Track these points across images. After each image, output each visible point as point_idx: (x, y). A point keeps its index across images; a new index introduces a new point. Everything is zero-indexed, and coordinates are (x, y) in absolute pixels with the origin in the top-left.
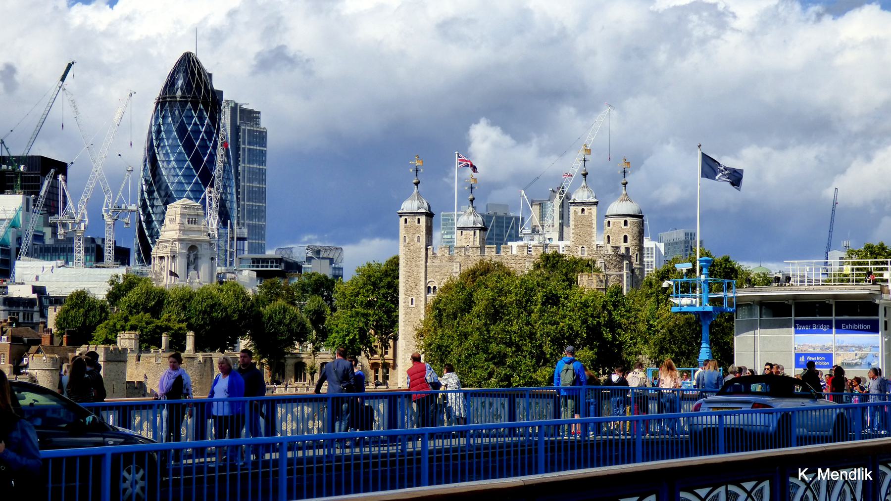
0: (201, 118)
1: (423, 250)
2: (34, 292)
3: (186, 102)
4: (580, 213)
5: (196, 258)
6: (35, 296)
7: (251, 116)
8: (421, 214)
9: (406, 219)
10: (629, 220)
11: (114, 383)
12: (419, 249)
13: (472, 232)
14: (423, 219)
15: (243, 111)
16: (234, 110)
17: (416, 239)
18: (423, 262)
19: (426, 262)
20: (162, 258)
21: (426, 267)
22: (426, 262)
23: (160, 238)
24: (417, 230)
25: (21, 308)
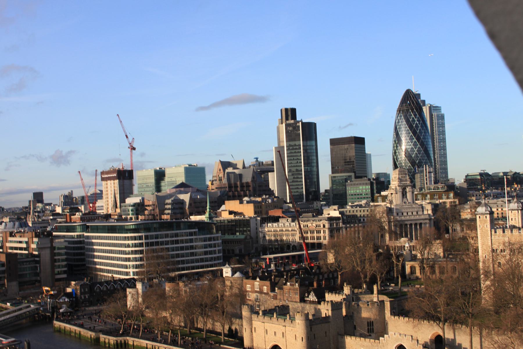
1: (489, 232)
2: (340, 214)
3: (409, 110)
6: (340, 216)
7: (437, 109)
8: (487, 214)
9: (480, 217)
11: (337, 320)
12: (487, 231)
13: (517, 211)
14: (488, 216)
15: (434, 107)
16: (430, 108)
17: (485, 226)
18: (490, 238)
19: (491, 237)
20: (392, 194)
21: (491, 240)
22: (491, 237)
24: (485, 222)
25: (335, 221)
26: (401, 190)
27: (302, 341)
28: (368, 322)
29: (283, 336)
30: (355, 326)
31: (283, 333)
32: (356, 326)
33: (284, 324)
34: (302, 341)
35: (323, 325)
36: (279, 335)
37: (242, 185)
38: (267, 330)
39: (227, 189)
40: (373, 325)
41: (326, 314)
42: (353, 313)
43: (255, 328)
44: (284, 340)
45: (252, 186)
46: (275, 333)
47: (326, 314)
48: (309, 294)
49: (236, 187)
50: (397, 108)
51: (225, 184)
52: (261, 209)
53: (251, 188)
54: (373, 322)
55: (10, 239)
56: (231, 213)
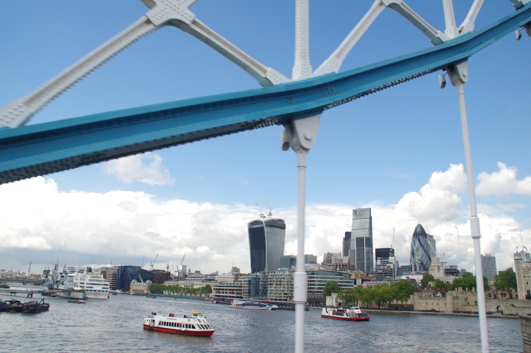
0: (423, 238)
5: (439, 270)
6: (407, 279)
20: (432, 270)
23: (431, 265)
26: (437, 268)
28: (475, 301)
29: (437, 304)
30: (469, 303)
31: (437, 303)
32: (469, 303)
33: (438, 299)
36: (435, 304)
38: (427, 303)
39: (335, 267)
41: (457, 296)
42: (467, 297)
43: (420, 303)
44: (438, 306)
45: (348, 266)
46: (433, 304)
47: (457, 296)
48: (437, 293)
49: (341, 266)
50: (413, 233)
51: (334, 264)
53: (348, 267)
55: (240, 277)
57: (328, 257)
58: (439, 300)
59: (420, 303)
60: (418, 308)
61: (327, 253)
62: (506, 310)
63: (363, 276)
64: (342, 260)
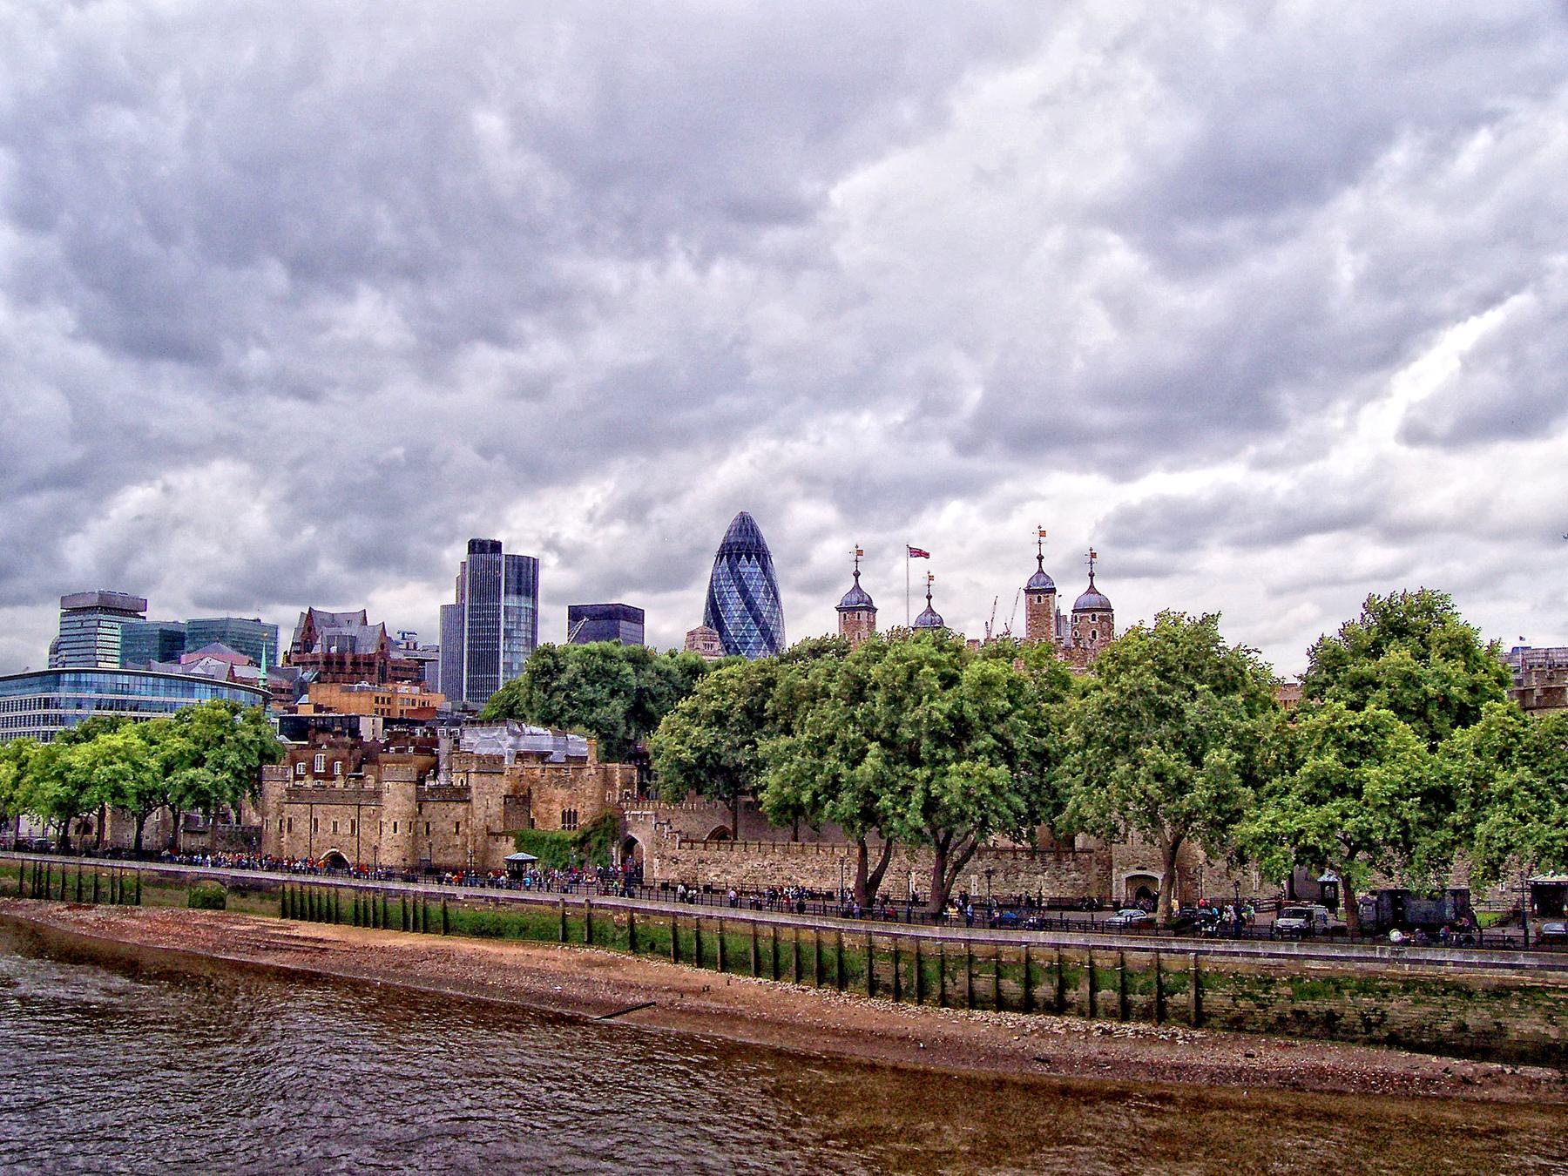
4: (1036, 602)
10: (1098, 614)
11: (487, 797)
17: (856, 637)
27: (395, 832)
28: (564, 813)
34: (395, 832)
35: (452, 805)
37: (355, 663)
38: (316, 820)
40: (575, 822)
41: (462, 781)
43: (290, 820)
47: (462, 781)
51: (316, 656)
52: (389, 707)
54: (575, 812)
56: (318, 708)
57: (310, 629)
58: (359, 805)
59: (290, 820)
60: (280, 848)
61: (307, 612)
62: (656, 861)
63: (414, 705)
64: (354, 639)
